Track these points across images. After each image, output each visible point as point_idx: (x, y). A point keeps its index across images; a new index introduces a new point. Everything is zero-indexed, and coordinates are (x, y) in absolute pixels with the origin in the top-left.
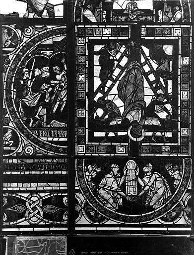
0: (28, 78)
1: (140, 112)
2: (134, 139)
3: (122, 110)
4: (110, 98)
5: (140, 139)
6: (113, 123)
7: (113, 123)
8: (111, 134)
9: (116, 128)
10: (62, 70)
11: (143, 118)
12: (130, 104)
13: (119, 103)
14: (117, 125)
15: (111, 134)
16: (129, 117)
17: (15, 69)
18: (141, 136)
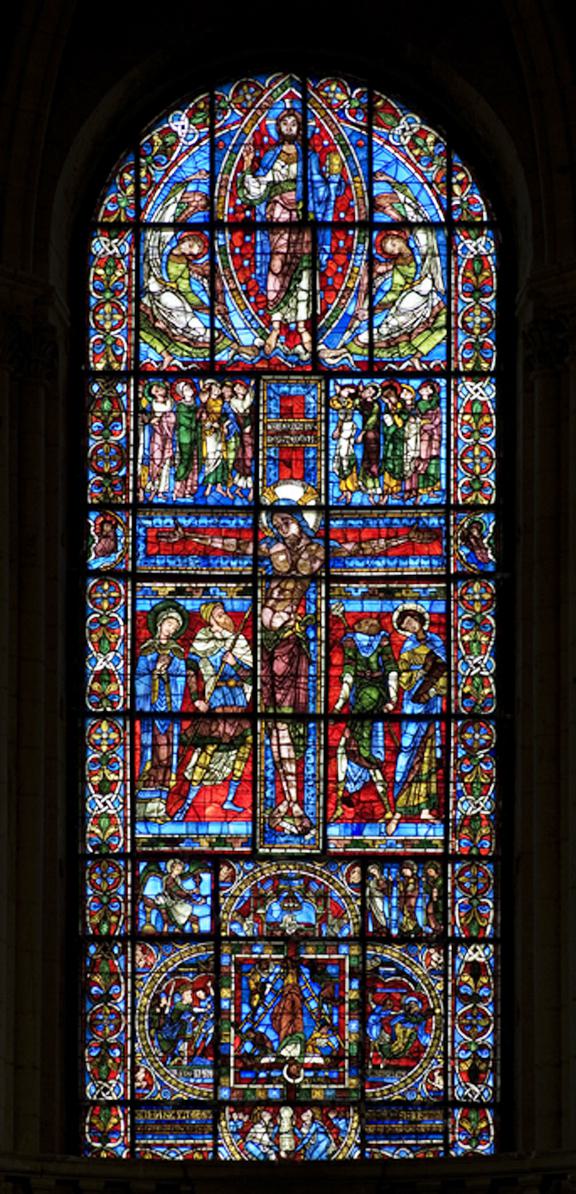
0: (165, 1006)
1: (299, 1046)
2: (291, 1080)
3: (276, 1044)
4: (261, 1029)
5: (298, 1081)
6: (265, 1060)
7: (265, 1060)
8: (262, 1075)
9: (269, 1067)
10: (208, 995)
11: (303, 1053)
12: (286, 1037)
13: (271, 1035)
14: (270, 1064)
15: (262, 1075)
16: (284, 1053)
17: (150, 994)
18: (298, 1077)
